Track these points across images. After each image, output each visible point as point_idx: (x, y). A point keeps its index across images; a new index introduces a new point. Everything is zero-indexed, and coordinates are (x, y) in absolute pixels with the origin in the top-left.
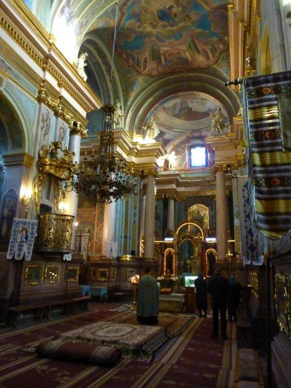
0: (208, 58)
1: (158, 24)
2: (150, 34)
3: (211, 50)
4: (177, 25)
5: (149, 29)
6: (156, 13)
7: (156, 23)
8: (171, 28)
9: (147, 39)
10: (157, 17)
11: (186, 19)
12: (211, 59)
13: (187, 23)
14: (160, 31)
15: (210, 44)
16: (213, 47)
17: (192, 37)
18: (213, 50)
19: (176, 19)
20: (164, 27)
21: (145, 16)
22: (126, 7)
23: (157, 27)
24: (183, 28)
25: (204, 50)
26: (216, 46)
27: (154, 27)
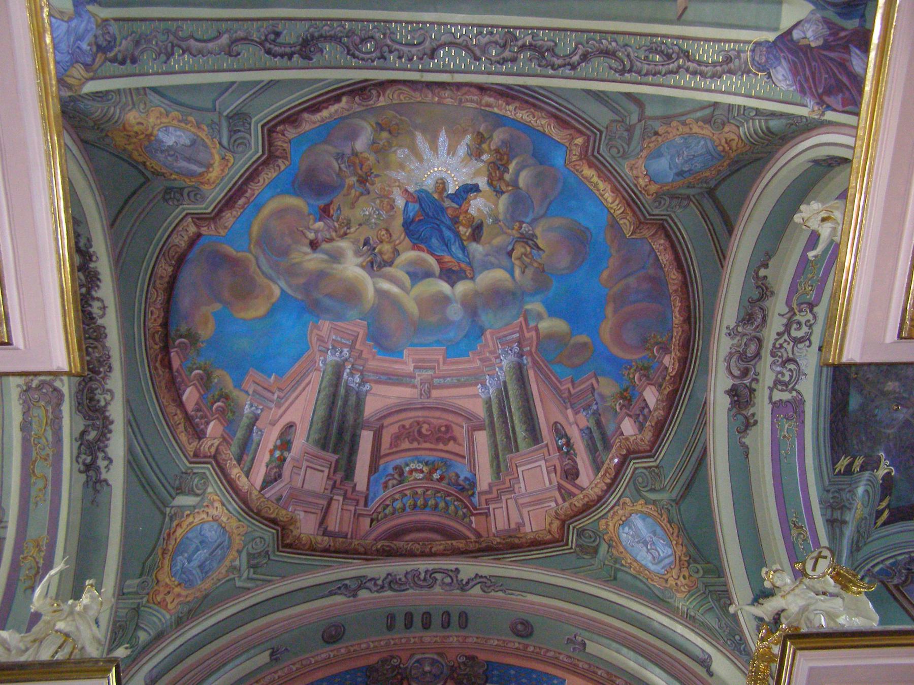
0: (572, 474)
1: (396, 252)
2: (350, 294)
3: (587, 433)
4: (472, 279)
5: (352, 268)
6: (400, 202)
7: (387, 247)
8: (445, 287)
9: (325, 325)
10: (399, 221)
11: (519, 250)
12: (584, 479)
13: (517, 272)
14: (394, 289)
15: (587, 407)
16: (599, 423)
17: (521, 355)
18: (597, 435)
19: (477, 249)
20: (418, 274)
21: (353, 206)
22: (291, 133)
23: (387, 269)
24: (499, 298)
25: (559, 431)
26: (610, 428)
27: (376, 264)
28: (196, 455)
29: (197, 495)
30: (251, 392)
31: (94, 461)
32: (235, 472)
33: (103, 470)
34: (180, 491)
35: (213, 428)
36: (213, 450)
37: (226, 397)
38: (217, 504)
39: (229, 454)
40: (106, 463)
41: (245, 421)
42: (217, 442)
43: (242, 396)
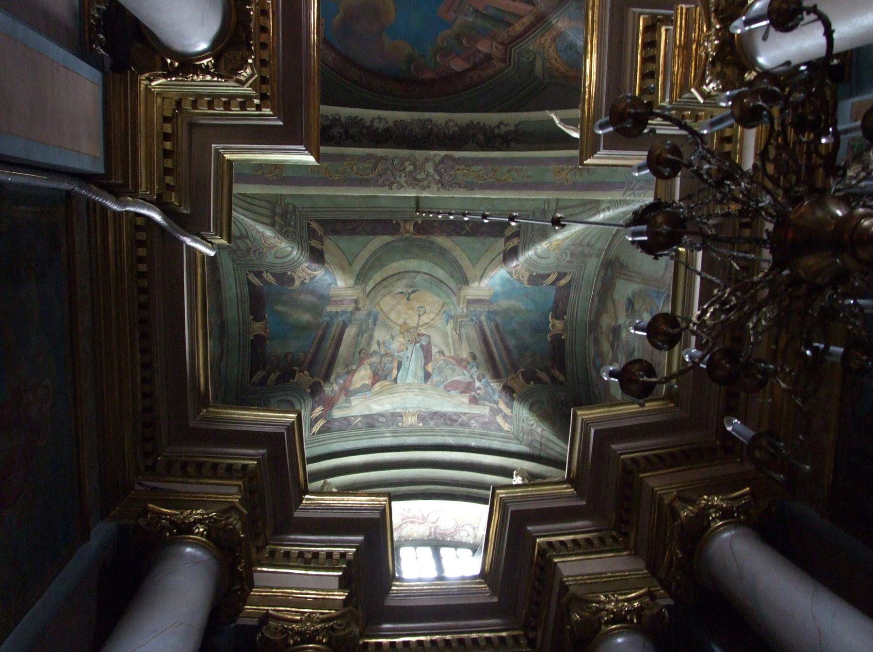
28: (504, 61)
29: (535, 58)
30: (455, 15)
31: (500, 136)
32: (518, 27)
33: (508, 128)
34: (532, 72)
35: (484, 47)
36: (500, 47)
37: (458, 37)
38: (543, 40)
39: (503, 34)
40: (502, 127)
41: (480, 22)
42: (495, 44)
43: (459, 22)
